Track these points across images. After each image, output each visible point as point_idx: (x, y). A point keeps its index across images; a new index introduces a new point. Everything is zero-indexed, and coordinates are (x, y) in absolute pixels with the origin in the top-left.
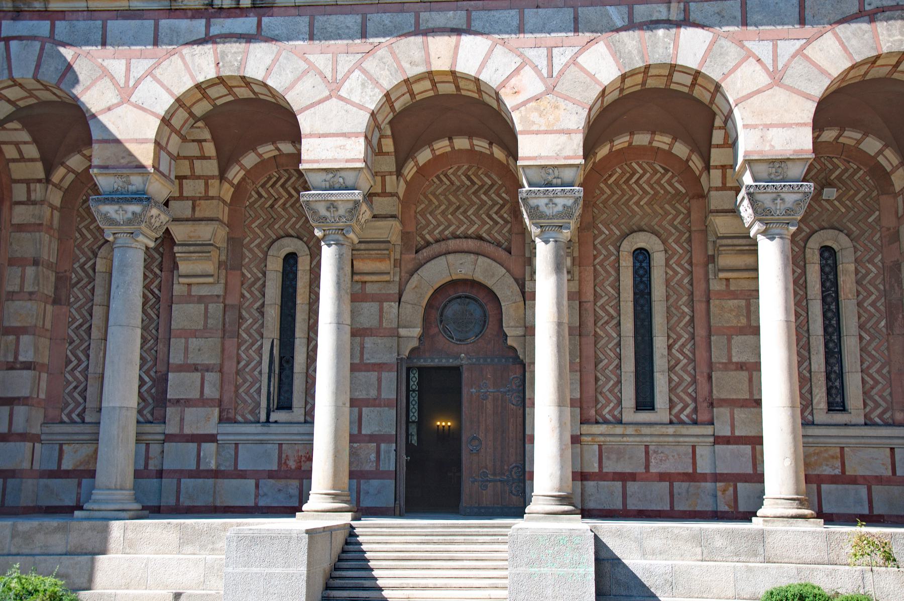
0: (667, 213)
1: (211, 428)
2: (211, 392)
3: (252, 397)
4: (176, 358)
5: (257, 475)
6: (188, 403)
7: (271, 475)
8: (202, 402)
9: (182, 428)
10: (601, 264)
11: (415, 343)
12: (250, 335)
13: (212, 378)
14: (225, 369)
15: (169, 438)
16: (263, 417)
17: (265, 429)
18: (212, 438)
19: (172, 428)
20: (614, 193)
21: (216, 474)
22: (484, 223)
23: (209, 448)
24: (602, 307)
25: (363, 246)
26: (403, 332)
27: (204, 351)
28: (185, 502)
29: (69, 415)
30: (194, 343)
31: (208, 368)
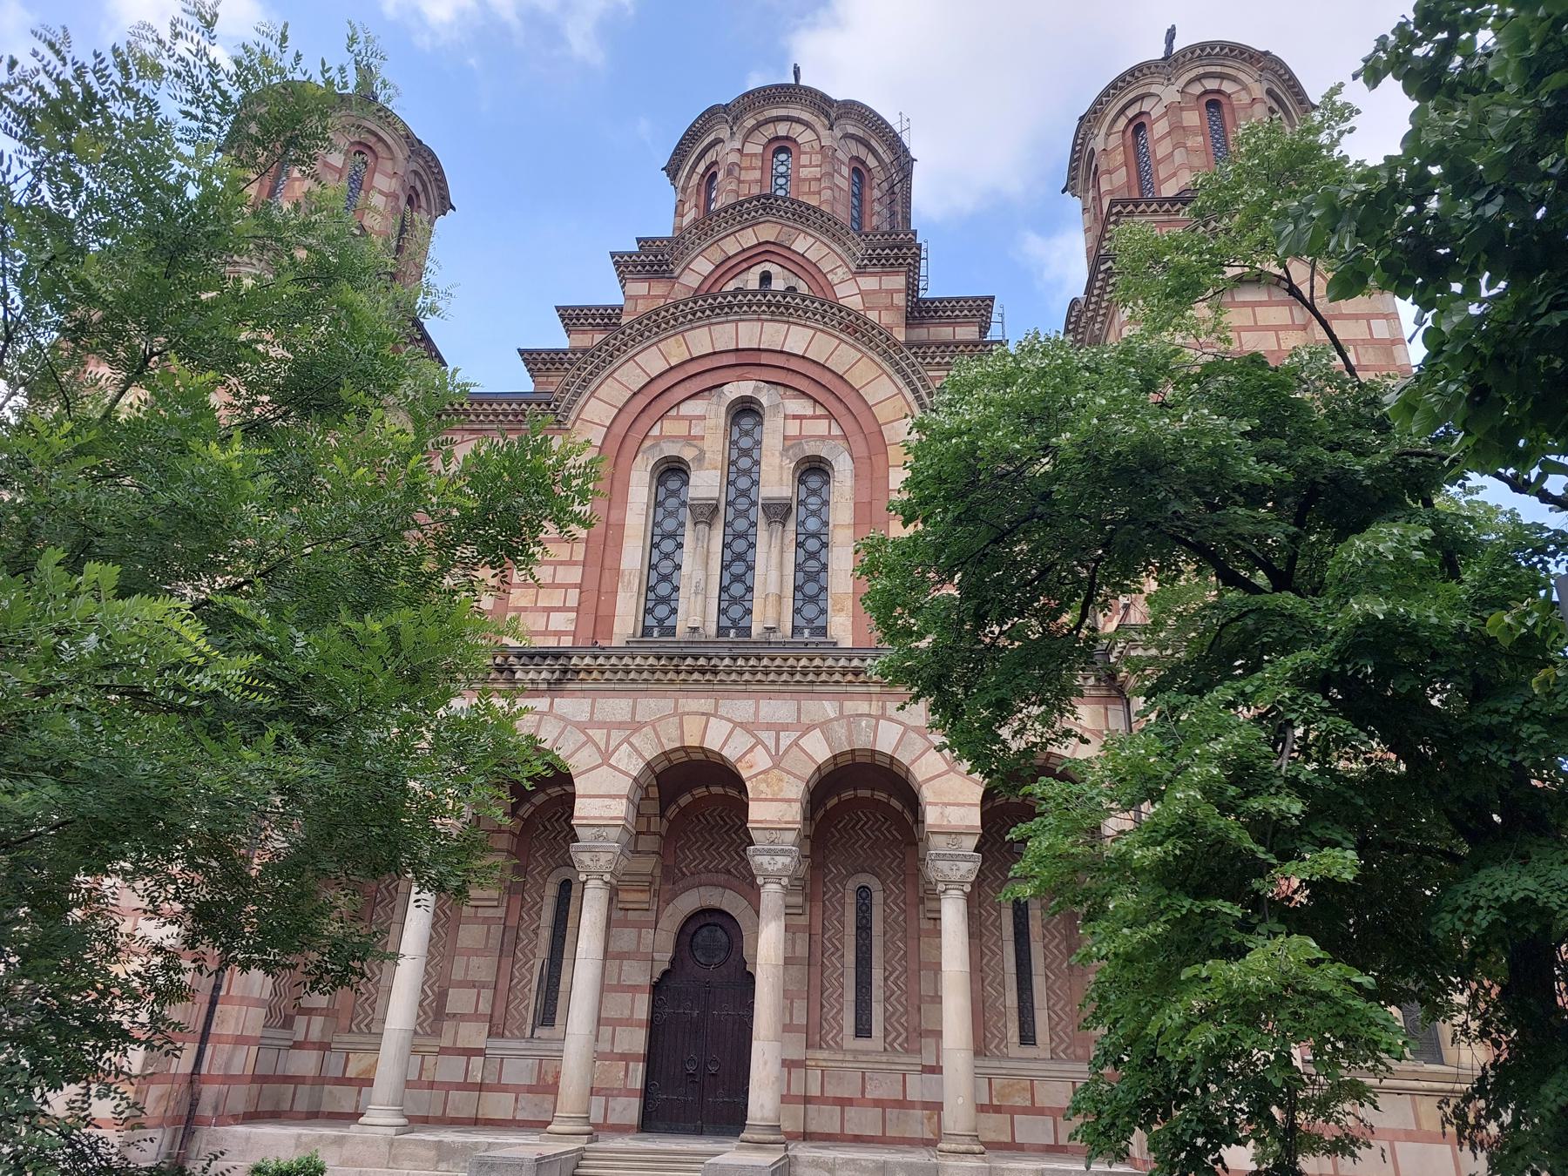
0: (886, 856)
1: (480, 1041)
2: (484, 1008)
3: (520, 1013)
4: (458, 975)
5: (517, 1090)
6: (463, 1017)
7: (530, 1089)
8: (476, 1017)
9: (455, 1042)
10: (829, 900)
11: (666, 966)
12: (525, 955)
13: (487, 994)
14: (499, 986)
15: (443, 1051)
16: (528, 1033)
17: (529, 1045)
18: (479, 1052)
19: (446, 1042)
20: (842, 837)
21: (480, 1087)
22: (733, 859)
23: (477, 1061)
24: (830, 940)
25: (627, 878)
26: (657, 956)
27: (482, 968)
28: (451, 1113)
29: (358, 1026)
30: (475, 961)
31: (484, 986)
